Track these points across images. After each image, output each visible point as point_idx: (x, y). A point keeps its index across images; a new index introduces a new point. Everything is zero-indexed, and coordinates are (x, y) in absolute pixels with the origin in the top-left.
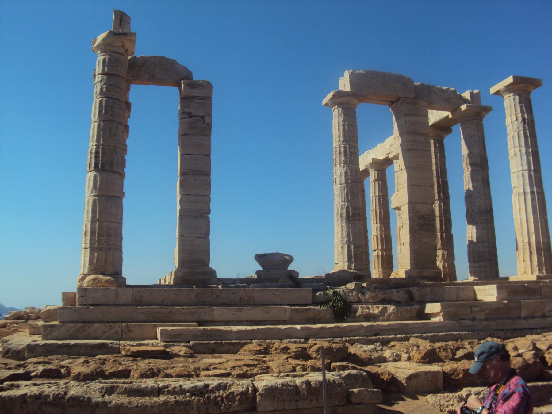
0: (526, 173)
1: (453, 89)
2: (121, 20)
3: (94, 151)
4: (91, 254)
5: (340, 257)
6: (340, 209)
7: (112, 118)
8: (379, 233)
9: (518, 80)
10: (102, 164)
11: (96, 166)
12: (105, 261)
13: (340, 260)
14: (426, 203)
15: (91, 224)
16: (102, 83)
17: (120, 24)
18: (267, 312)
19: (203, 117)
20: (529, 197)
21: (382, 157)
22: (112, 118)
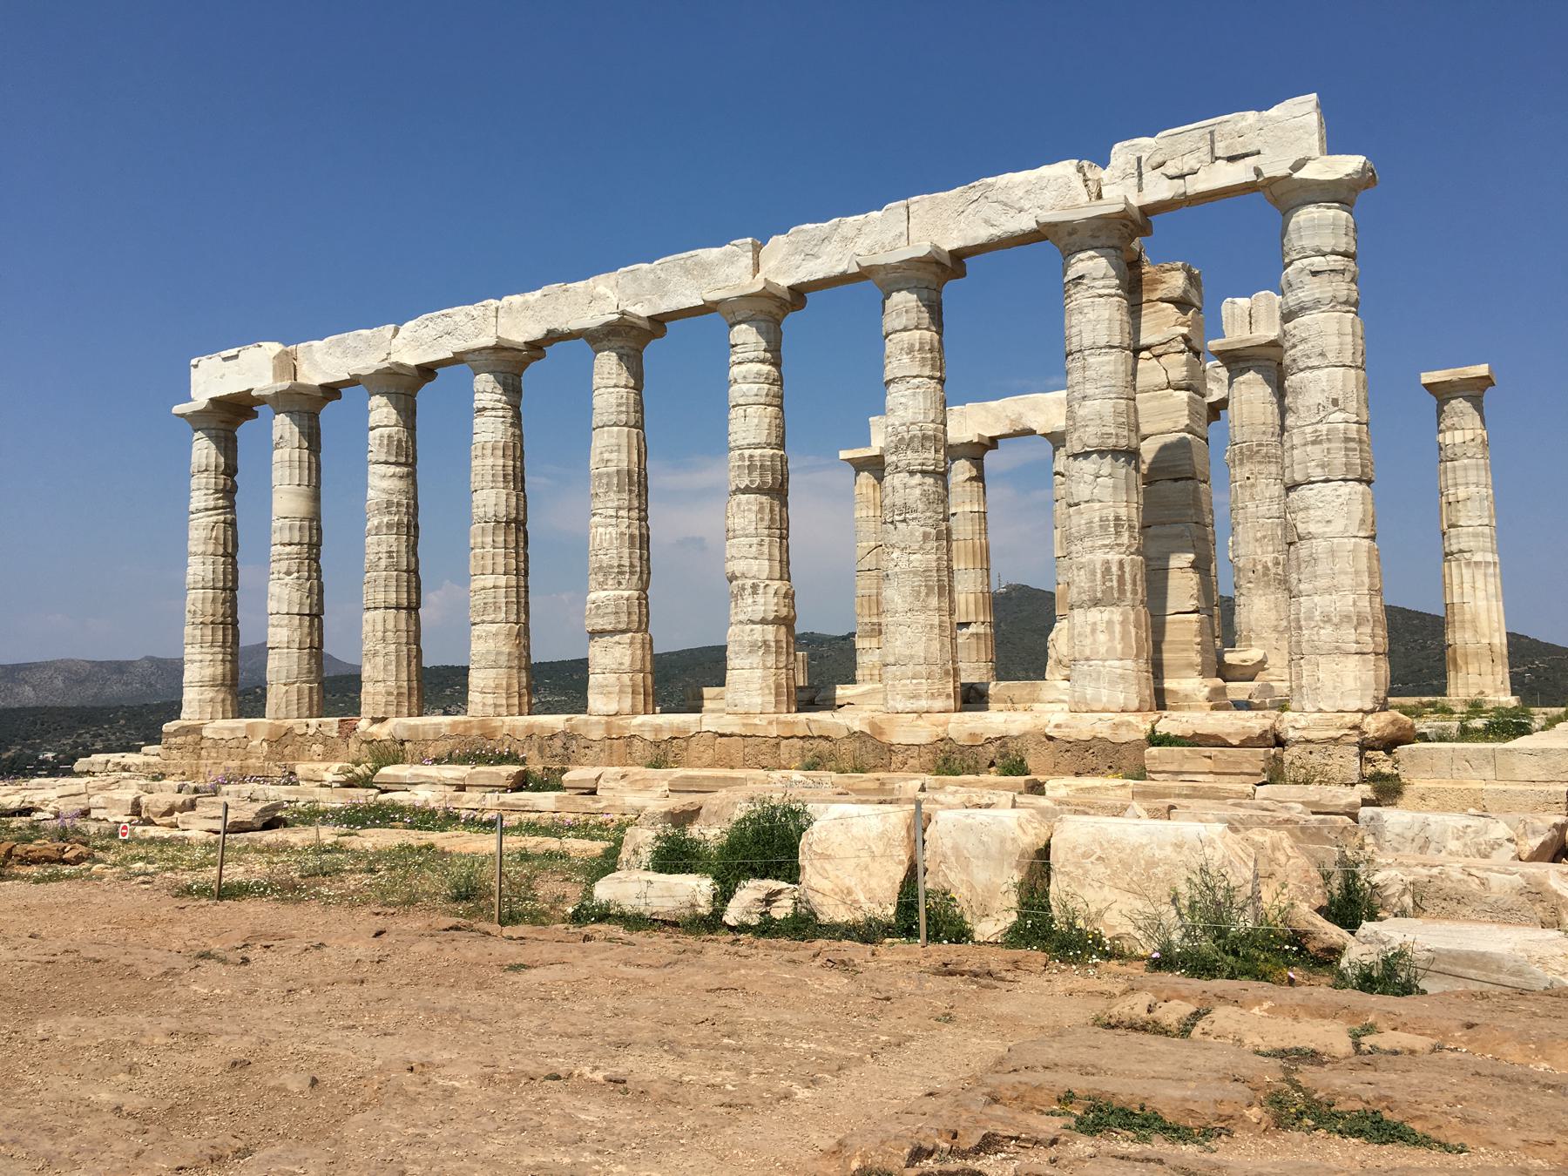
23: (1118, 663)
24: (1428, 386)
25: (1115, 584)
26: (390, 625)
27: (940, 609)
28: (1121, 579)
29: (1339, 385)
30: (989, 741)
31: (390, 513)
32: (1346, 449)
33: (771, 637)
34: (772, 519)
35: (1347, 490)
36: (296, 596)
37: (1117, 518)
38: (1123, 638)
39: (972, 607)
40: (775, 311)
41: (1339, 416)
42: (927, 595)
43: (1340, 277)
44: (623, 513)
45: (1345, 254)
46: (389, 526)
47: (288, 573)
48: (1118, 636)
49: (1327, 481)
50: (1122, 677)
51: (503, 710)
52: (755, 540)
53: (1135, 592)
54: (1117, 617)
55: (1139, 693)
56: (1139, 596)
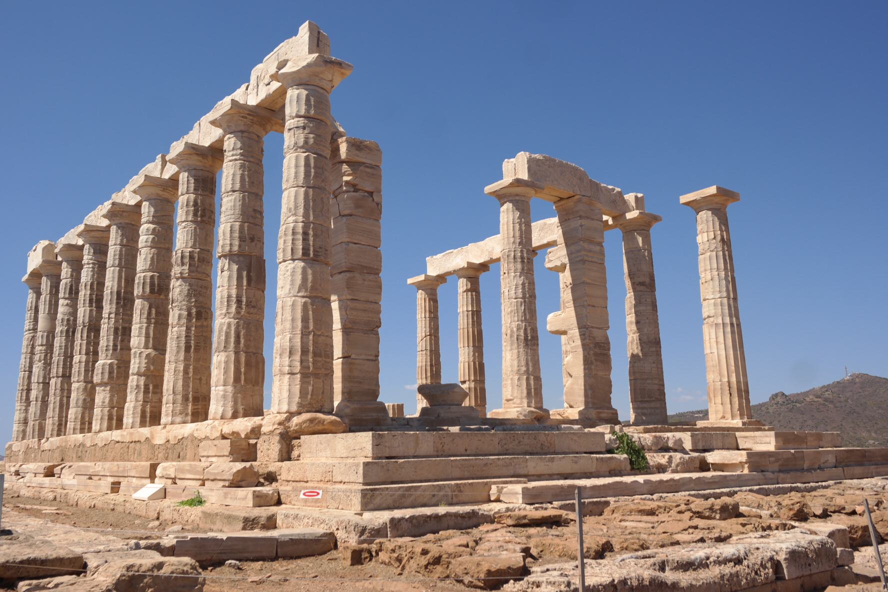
0: (725, 301)
1: (619, 190)
3: (300, 230)
4: (304, 382)
5: (516, 391)
6: (515, 329)
7: (323, 184)
8: (472, 359)
9: (723, 192)
10: (314, 251)
11: (305, 252)
12: (323, 393)
13: (515, 395)
15: (302, 338)
16: (306, 131)
17: (318, 45)
18: (576, 463)
20: (729, 329)
21: (478, 261)
22: (323, 184)
24: (687, 204)
25: (223, 338)
29: (293, 198)
30: (179, 441)
32: (293, 240)
35: (293, 266)
36: (42, 373)
37: (229, 296)
40: (161, 193)
42: (178, 352)
44: (113, 316)
47: (40, 361)
48: (223, 371)
49: (285, 261)
51: (78, 431)
52: (138, 326)
53: (237, 341)
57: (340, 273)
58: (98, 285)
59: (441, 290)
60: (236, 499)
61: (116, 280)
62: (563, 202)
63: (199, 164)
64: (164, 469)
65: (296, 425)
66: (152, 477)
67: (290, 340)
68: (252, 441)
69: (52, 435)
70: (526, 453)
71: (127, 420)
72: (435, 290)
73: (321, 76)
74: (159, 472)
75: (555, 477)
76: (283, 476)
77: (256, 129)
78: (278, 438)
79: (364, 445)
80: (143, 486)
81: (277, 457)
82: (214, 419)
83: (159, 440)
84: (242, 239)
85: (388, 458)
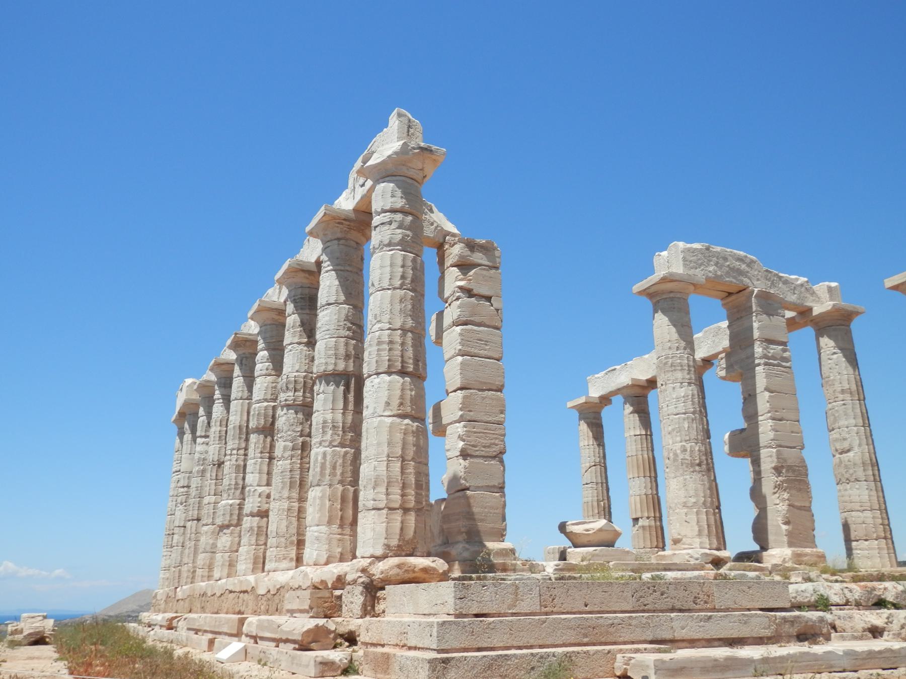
2: (409, 127)
6: (678, 452)
14: (794, 447)
18: (745, 623)
19: (488, 299)
23: (315, 528)
24: (895, 288)
25: (318, 469)
26: (194, 530)
27: (289, 498)
28: (323, 466)
30: (278, 590)
31: (198, 465)
32: (378, 350)
33: (255, 524)
34: (264, 447)
37: (325, 422)
38: (320, 510)
39: (639, 506)
40: (277, 317)
41: (378, 326)
42: (283, 488)
43: (387, 227)
44: (235, 452)
45: (393, 211)
46: (198, 472)
47: (181, 504)
48: (317, 508)
50: (317, 539)
51: (206, 579)
53: (333, 474)
54: (319, 494)
55: (329, 550)
56: (338, 477)
57: (455, 391)
58: (225, 422)
59: (607, 414)
60: (300, 665)
61: (239, 413)
62: (733, 297)
63: (305, 281)
64: (250, 624)
65: (382, 573)
66: (238, 635)
67: (375, 467)
68: (337, 593)
69: (186, 584)
70: (673, 610)
71: (241, 567)
72: (599, 413)
73: (410, 165)
74: (245, 629)
75: (716, 643)
76: (362, 638)
77: (354, 235)
78: (361, 588)
79: (446, 598)
80: (230, 643)
81: (360, 613)
82: (308, 565)
83: (261, 591)
84: (336, 356)
85: (477, 616)
